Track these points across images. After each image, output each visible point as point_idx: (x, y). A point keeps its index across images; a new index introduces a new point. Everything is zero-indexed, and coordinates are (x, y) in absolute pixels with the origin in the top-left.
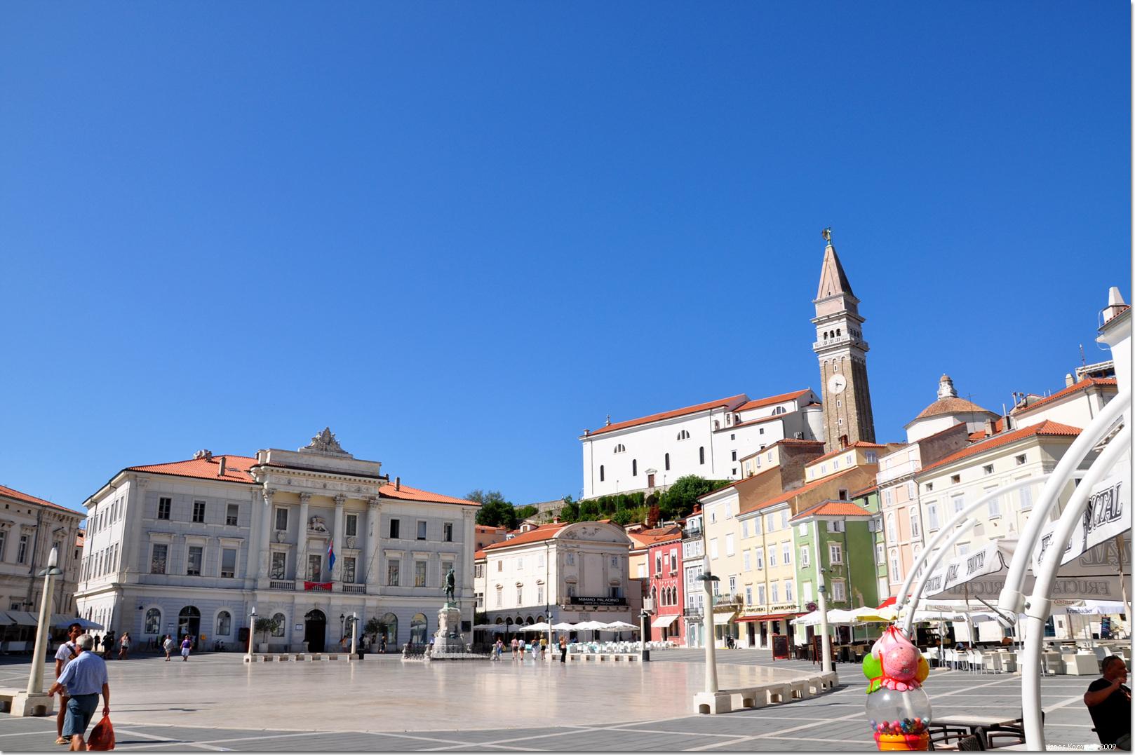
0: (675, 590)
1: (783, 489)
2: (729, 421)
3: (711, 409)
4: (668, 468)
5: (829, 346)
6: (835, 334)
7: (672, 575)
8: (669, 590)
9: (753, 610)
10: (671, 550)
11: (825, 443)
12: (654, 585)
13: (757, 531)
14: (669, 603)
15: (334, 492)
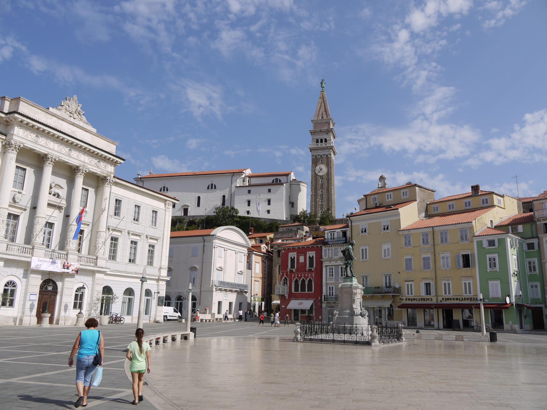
0: (310, 281)
1: (419, 217)
2: (244, 181)
3: (234, 173)
4: (199, 205)
5: (320, 147)
6: (324, 142)
7: (310, 271)
8: (303, 281)
9: (414, 299)
10: (308, 253)
11: (435, 191)
12: (285, 276)
13: (425, 242)
14: (303, 289)
15: (77, 161)
